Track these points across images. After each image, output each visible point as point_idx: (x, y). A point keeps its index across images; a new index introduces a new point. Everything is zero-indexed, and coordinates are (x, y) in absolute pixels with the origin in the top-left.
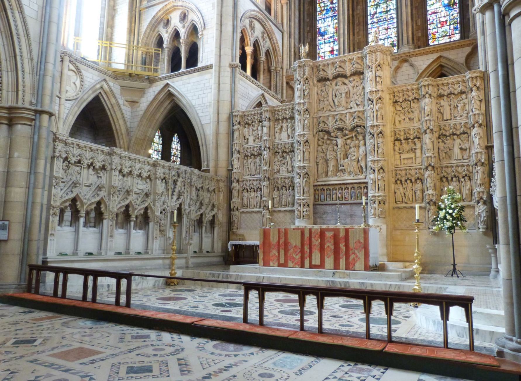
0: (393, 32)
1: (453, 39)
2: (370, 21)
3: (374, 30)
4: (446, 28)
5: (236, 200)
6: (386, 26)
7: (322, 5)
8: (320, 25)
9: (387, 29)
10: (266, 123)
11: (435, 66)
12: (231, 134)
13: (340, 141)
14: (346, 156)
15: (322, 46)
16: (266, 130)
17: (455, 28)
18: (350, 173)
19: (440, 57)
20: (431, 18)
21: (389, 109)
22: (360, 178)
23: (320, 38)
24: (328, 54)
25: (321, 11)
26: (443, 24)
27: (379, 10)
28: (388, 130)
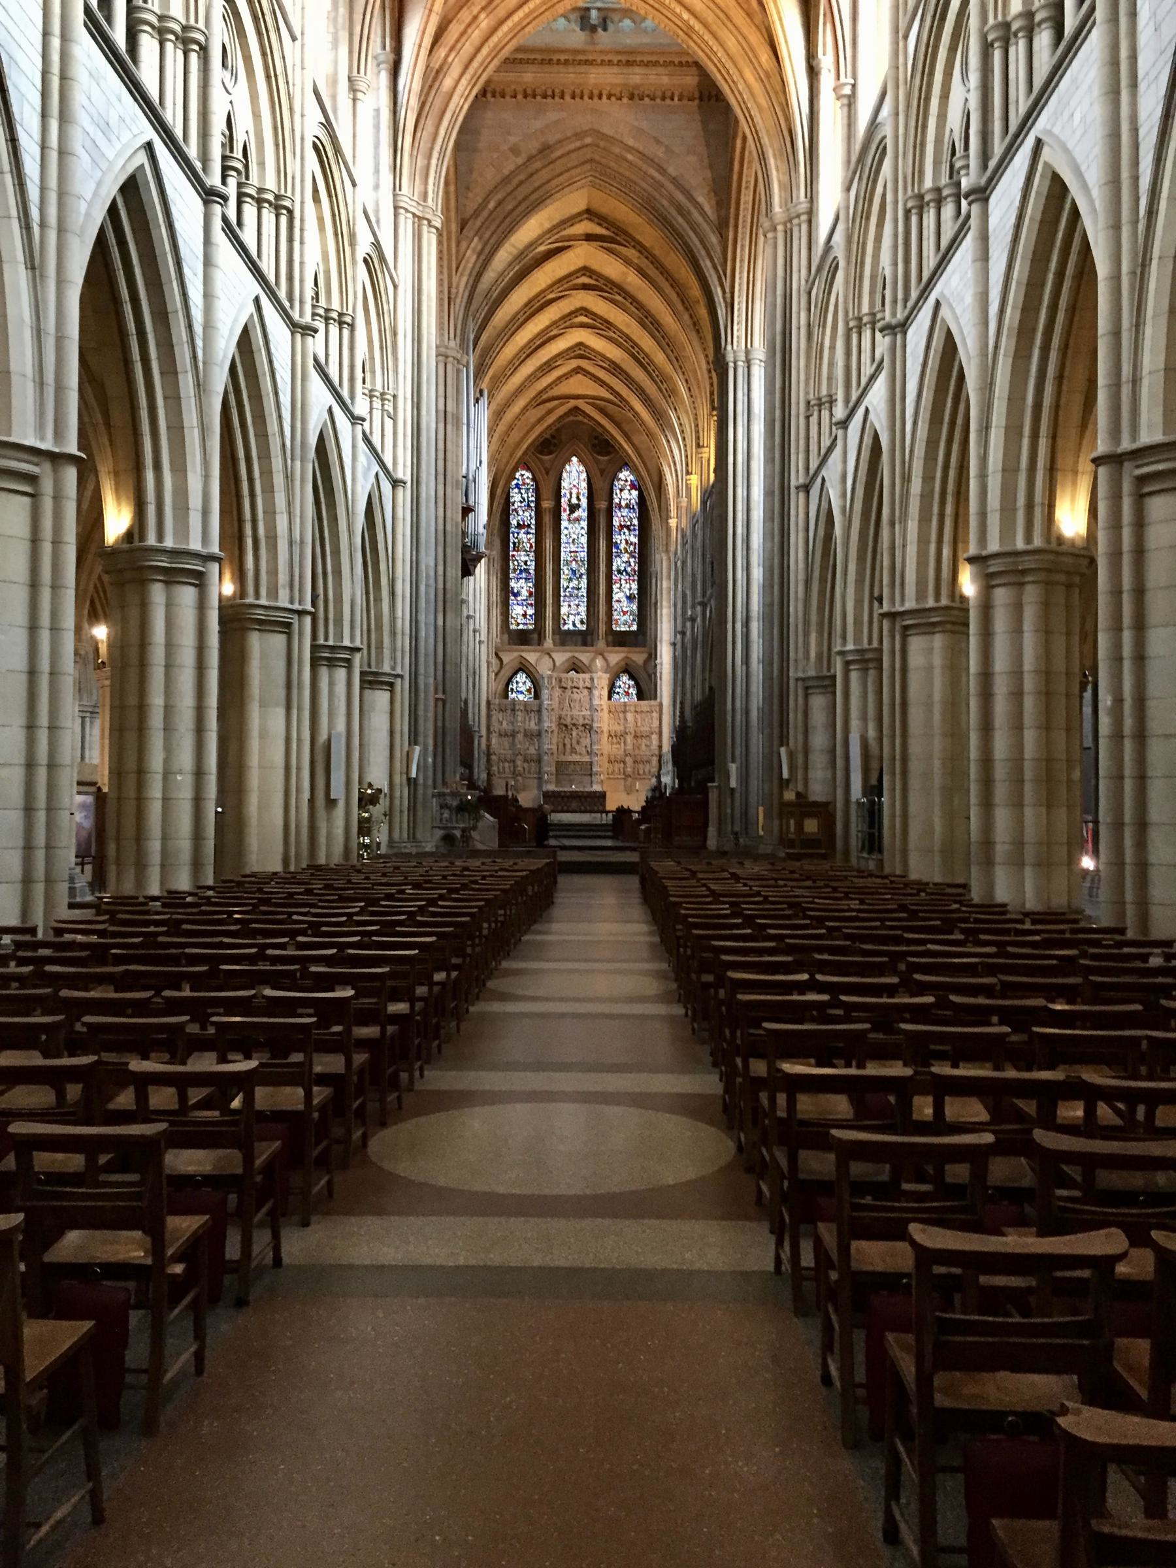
0: (583, 609)
2: (562, 594)
4: (626, 617)
5: (495, 768)
8: (512, 584)
9: (578, 606)
10: (519, 713)
11: (623, 663)
12: (489, 716)
13: (574, 734)
19: (627, 657)
20: (615, 605)
22: (587, 759)
24: (520, 617)
25: (515, 570)
26: (625, 613)
27: (571, 585)
28: (605, 729)
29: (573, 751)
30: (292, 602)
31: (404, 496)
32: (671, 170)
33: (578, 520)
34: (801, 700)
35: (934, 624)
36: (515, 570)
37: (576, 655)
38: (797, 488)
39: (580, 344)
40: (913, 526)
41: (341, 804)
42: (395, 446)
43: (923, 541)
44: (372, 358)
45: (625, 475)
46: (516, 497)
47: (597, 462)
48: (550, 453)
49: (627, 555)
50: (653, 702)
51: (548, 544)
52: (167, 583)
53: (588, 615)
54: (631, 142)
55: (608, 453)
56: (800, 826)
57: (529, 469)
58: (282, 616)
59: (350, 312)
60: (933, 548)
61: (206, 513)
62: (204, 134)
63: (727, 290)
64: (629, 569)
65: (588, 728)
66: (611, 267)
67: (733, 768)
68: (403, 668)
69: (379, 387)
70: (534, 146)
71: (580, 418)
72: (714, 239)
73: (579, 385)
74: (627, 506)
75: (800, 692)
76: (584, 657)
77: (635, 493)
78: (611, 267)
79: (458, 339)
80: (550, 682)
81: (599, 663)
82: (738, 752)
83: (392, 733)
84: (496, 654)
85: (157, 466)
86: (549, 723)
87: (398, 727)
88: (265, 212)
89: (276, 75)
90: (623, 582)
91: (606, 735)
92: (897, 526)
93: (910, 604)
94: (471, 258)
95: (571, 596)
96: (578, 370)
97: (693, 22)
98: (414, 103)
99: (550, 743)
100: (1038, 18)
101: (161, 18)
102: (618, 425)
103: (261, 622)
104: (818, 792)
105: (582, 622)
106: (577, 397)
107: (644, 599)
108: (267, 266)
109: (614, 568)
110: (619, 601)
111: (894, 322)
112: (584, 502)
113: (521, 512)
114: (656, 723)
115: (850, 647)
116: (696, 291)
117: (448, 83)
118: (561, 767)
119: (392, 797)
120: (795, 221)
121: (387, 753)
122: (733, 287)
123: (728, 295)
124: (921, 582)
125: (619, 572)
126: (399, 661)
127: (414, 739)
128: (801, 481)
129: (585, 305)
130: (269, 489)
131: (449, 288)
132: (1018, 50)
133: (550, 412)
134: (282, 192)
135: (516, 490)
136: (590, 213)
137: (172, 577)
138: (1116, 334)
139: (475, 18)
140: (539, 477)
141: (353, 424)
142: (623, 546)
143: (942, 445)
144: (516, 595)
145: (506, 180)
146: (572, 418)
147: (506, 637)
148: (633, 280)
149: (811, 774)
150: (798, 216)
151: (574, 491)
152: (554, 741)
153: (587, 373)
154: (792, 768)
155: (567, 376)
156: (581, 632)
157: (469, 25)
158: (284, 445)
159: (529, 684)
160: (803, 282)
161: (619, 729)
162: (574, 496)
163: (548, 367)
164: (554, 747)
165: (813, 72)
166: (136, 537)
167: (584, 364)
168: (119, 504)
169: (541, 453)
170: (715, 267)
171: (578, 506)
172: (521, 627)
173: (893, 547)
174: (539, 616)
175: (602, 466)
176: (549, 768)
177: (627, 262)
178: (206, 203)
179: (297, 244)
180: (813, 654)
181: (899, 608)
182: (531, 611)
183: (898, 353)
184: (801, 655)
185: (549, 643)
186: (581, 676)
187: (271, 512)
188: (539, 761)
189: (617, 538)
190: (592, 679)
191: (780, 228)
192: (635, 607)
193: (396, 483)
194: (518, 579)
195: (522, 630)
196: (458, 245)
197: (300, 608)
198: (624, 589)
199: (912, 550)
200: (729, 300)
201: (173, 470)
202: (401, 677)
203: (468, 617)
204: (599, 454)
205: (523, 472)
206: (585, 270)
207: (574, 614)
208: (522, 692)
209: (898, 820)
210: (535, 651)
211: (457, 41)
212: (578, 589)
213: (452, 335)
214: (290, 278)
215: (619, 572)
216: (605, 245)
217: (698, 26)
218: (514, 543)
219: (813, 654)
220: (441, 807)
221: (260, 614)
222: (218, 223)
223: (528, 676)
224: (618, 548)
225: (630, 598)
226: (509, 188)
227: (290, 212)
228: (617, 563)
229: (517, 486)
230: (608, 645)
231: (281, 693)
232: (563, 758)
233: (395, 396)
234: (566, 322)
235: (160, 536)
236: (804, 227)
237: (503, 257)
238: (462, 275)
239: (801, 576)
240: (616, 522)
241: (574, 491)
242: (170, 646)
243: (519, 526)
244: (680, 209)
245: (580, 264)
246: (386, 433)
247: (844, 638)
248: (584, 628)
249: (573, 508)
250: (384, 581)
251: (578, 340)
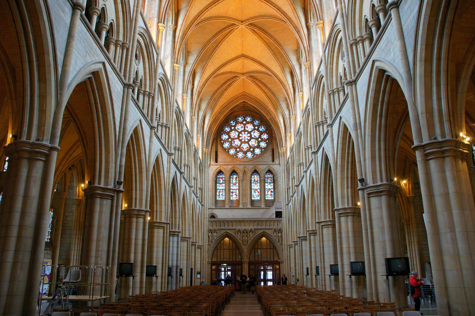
88: (163, 128)
100: (340, 89)
108: (163, 141)
132: (336, 96)
138: (360, 162)
183: (316, 159)
197: (167, 222)
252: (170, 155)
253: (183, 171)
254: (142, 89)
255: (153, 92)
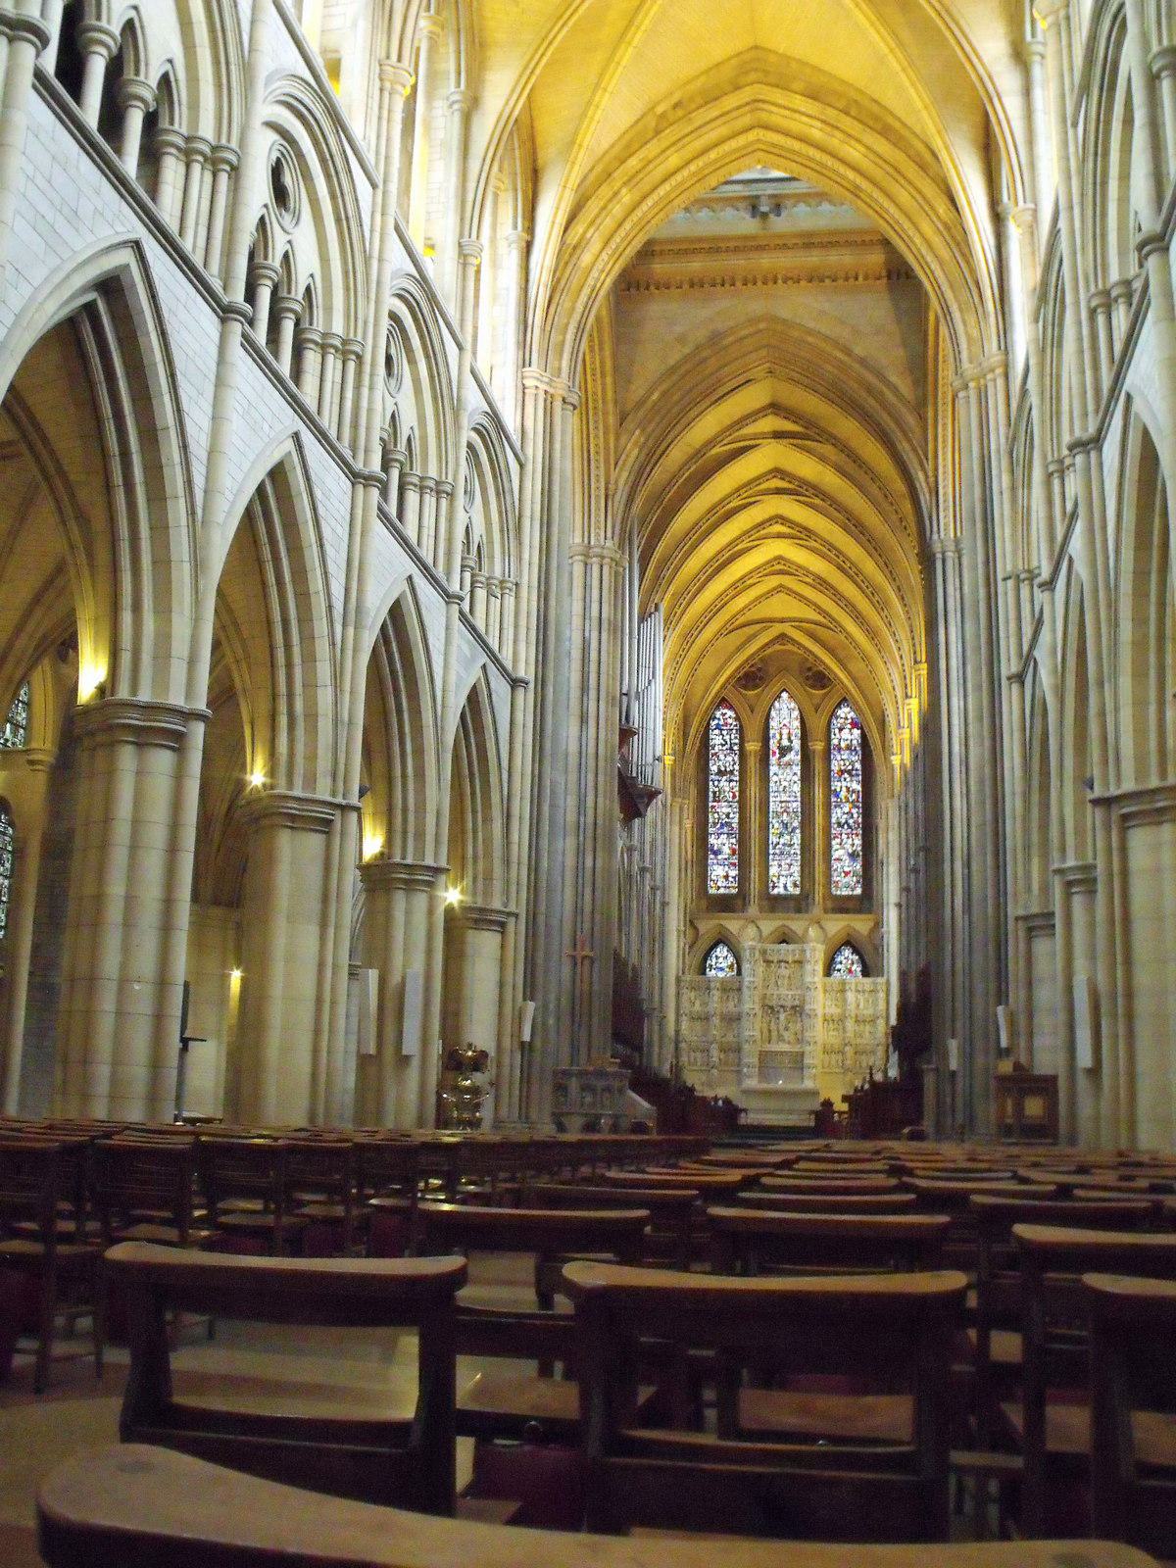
0: (796, 869)
1: (855, 893)
2: (771, 852)
3: (776, 863)
5: (684, 1059)
6: (788, 861)
7: (716, 815)
8: (712, 840)
10: (715, 992)
13: (782, 1016)
14: (786, 1029)
15: (715, 867)
16: (716, 998)
17: (858, 882)
18: (789, 1043)
19: (848, 926)
20: (835, 865)
21: (822, 995)
22: (797, 1049)
23: (712, 856)
25: (715, 824)
27: (782, 841)
29: (780, 1038)
30: (334, 795)
31: (526, 699)
32: (858, 350)
33: (789, 764)
34: (1022, 946)
35: (1161, 811)
36: (715, 824)
37: (786, 923)
38: (1009, 678)
39: (779, 559)
40: (1126, 682)
41: (415, 1063)
42: (515, 641)
43: (1140, 703)
44: (491, 542)
45: (844, 712)
46: (716, 739)
47: (811, 696)
48: (756, 687)
49: (847, 805)
50: (880, 980)
51: (753, 790)
52: (140, 745)
53: (802, 876)
54: (811, 325)
55: (823, 687)
56: (1019, 1108)
57: (731, 708)
58: (324, 812)
59: (450, 480)
60: (1153, 709)
61: (192, 662)
62: (228, 253)
63: (930, 474)
64: (851, 821)
65: (798, 1011)
66: (806, 467)
67: (953, 1045)
68: (519, 905)
69: (498, 573)
70: (701, 335)
71: (789, 647)
72: (911, 420)
73: (780, 607)
74: (848, 748)
75: (1022, 934)
76: (796, 925)
77: (857, 732)
78: (806, 467)
79: (616, 538)
80: (753, 954)
81: (812, 932)
82: (959, 1025)
83: (501, 985)
84: (691, 922)
85: (137, 608)
86: (750, 1003)
87: (509, 979)
88: (330, 358)
89: (347, 218)
90: (844, 836)
91: (820, 1019)
92: (1106, 686)
93: (1129, 785)
94: (632, 454)
95: (782, 853)
96: (780, 589)
97: (859, 180)
98: (546, 277)
99: (752, 1029)
101: (188, 139)
102: (831, 651)
103: (293, 818)
104: (1047, 1059)
105: (795, 885)
106: (782, 621)
107: (868, 855)
109: (834, 820)
110: (839, 859)
111: (1085, 437)
112: (797, 744)
113: (722, 757)
114: (882, 1006)
115: (1071, 863)
116: (899, 486)
117: (587, 258)
118: (765, 1058)
119: (499, 1065)
120: (989, 376)
121: (494, 1009)
122: (936, 469)
123: (932, 479)
124: (1141, 759)
125: (840, 825)
126: (513, 895)
127: (530, 991)
128: (1014, 669)
129: (780, 512)
130: (310, 658)
131: (607, 483)
133: (750, 639)
134: (352, 336)
135: (717, 732)
136: (775, 408)
137: (144, 739)
139: (616, 194)
140: (744, 716)
141: (447, 603)
142: (843, 794)
143: (1154, 577)
144: (717, 853)
145: (673, 370)
146: (777, 647)
147: (704, 903)
148: (830, 479)
149: (1038, 1042)
150: (992, 371)
151: (785, 732)
152: (757, 1027)
153: (790, 592)
154: (1013, 1034)
155: (769, 594)
156: (791, 897)
157: (610, 200)
158: (330, 607)
159: (731, 959)
160: (1003, 440)
161: (835, 1011)
162: (785, 737)
163: (738, 587)
164: (757, 1033)
165: (998, 219)
166: (108, 692)
167: (787, 581)
168: (96, 651)
169: (745, 687)
170: (914, 450)
171: (790, 749)
172: (722, 891)
173: (1102, 714)
174: (743, 879)
175: (816, 701)
176: (751, 1058)
177: (823, 459)
178: (223, 321)
179: (365, 391)
180: (1035, 886)
181: (1114, 791)
182: (733, 873)
184: (1021, 883)
185: (753, 910)
186: (791, 947)
187: (310, 685)
188: (738, 1050)
189: (836, 785)
190: (803, 951)
191: (972, 385)
192: (858, 867)
193: (515, 683)
194: (719, 835)
195: (724, 895)
196: (617, 439)
197: (344, 802)
198: (845, 848)
199: (1126, 714)
200: (932, 485)
201: (156, 611)
202: (517, 916)
203: (643, 870)
204: (813, 687)
205: (725, 711)
206: (778, 472)
207: (785, 876)
208: (722, 969)
209: (1123, 1080)
210: (739, 918)
211: (597, 216)
212: (791, 845)
213: (609, 534)
214: (355, 425)
215: (840, 825)
216: (795, 441)
217: (864, 184)
218: (714, 793)
219: (1035, 886)
220: (583, 1089)
221: (293, 807)
222: (236, 339)
223: (730, 950)
224: (837, 796)
225: (853, 856)
226: (675, 378)
227: (359, 357)
228: (837, 814)
229: (718, 727)
230: (826, 911)
231: (315, 906)
232: (768, 1047)
233: (517, 584)
234: (756, 534)
235: (134, 688)
236: (1000, 382)
237: (676, 455)
238: (621, 470)
239: (1018, 789)
240: (835, 767)
241: (785, 732)
242: (137, 823)
243: (720, 773)
244: (870, 390)
245: (770, 466)
246: (505, 626)
247: (1063, 850)
248: (797, 891)
249: (784, 751)
250: (495, 798)
251: (777, 553)
252: (365, 486)
253: (455, 587)
254: (176, 127)
255: (234, 145)
